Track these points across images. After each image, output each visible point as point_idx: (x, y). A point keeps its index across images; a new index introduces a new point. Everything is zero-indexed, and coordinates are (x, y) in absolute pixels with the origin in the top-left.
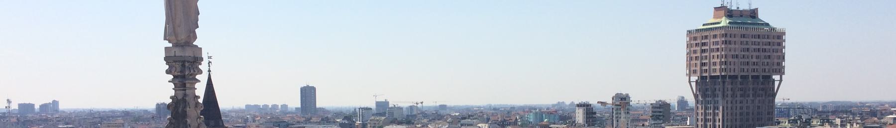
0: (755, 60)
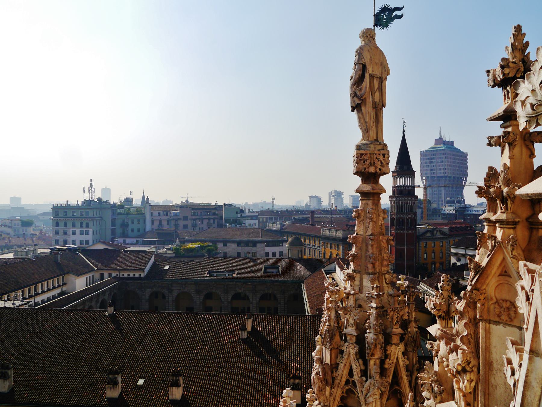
0: (457, 168)
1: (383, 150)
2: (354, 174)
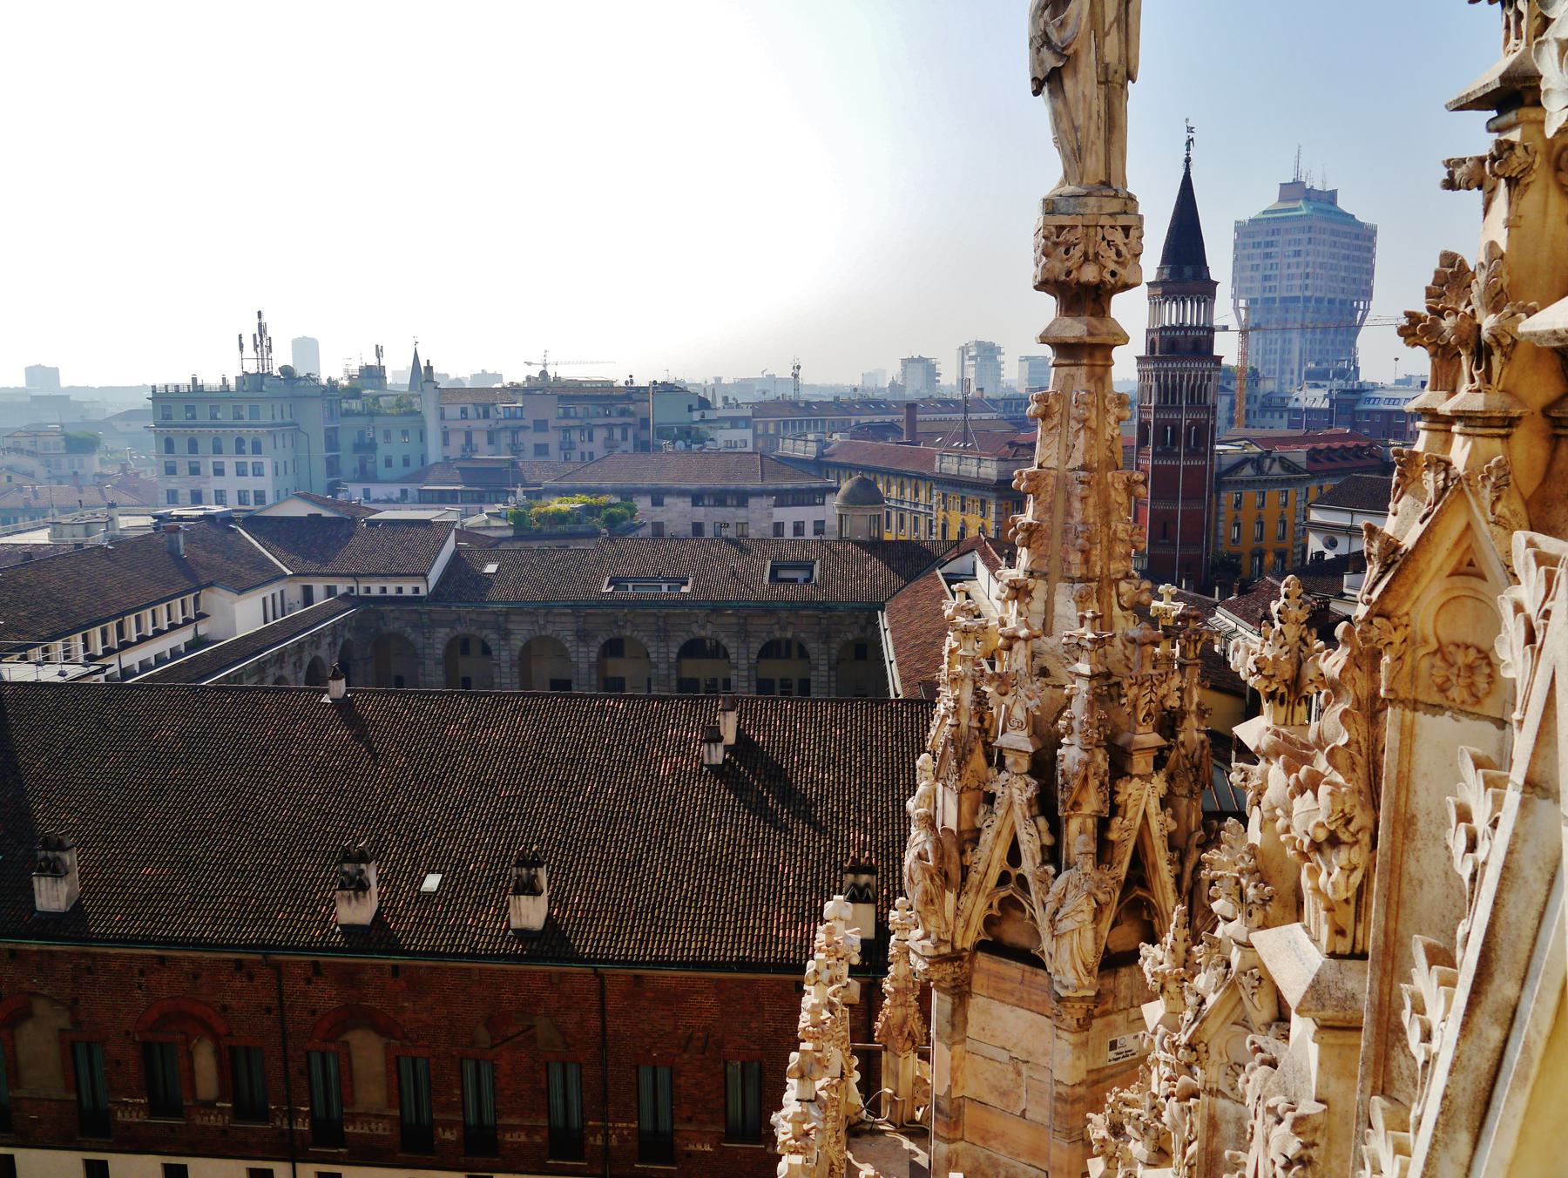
0: (1343, 274)
1: (1125, 213)
2: (1036, 288)
